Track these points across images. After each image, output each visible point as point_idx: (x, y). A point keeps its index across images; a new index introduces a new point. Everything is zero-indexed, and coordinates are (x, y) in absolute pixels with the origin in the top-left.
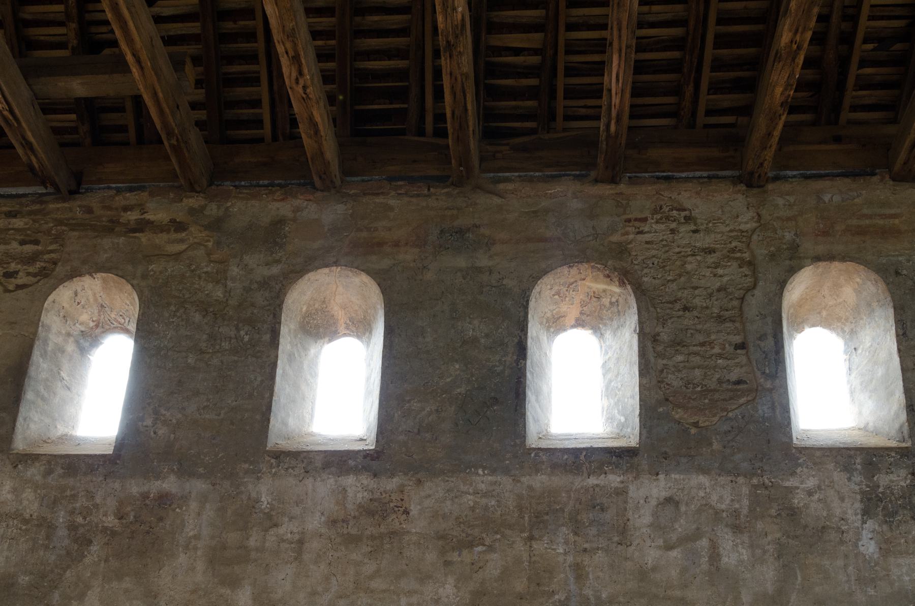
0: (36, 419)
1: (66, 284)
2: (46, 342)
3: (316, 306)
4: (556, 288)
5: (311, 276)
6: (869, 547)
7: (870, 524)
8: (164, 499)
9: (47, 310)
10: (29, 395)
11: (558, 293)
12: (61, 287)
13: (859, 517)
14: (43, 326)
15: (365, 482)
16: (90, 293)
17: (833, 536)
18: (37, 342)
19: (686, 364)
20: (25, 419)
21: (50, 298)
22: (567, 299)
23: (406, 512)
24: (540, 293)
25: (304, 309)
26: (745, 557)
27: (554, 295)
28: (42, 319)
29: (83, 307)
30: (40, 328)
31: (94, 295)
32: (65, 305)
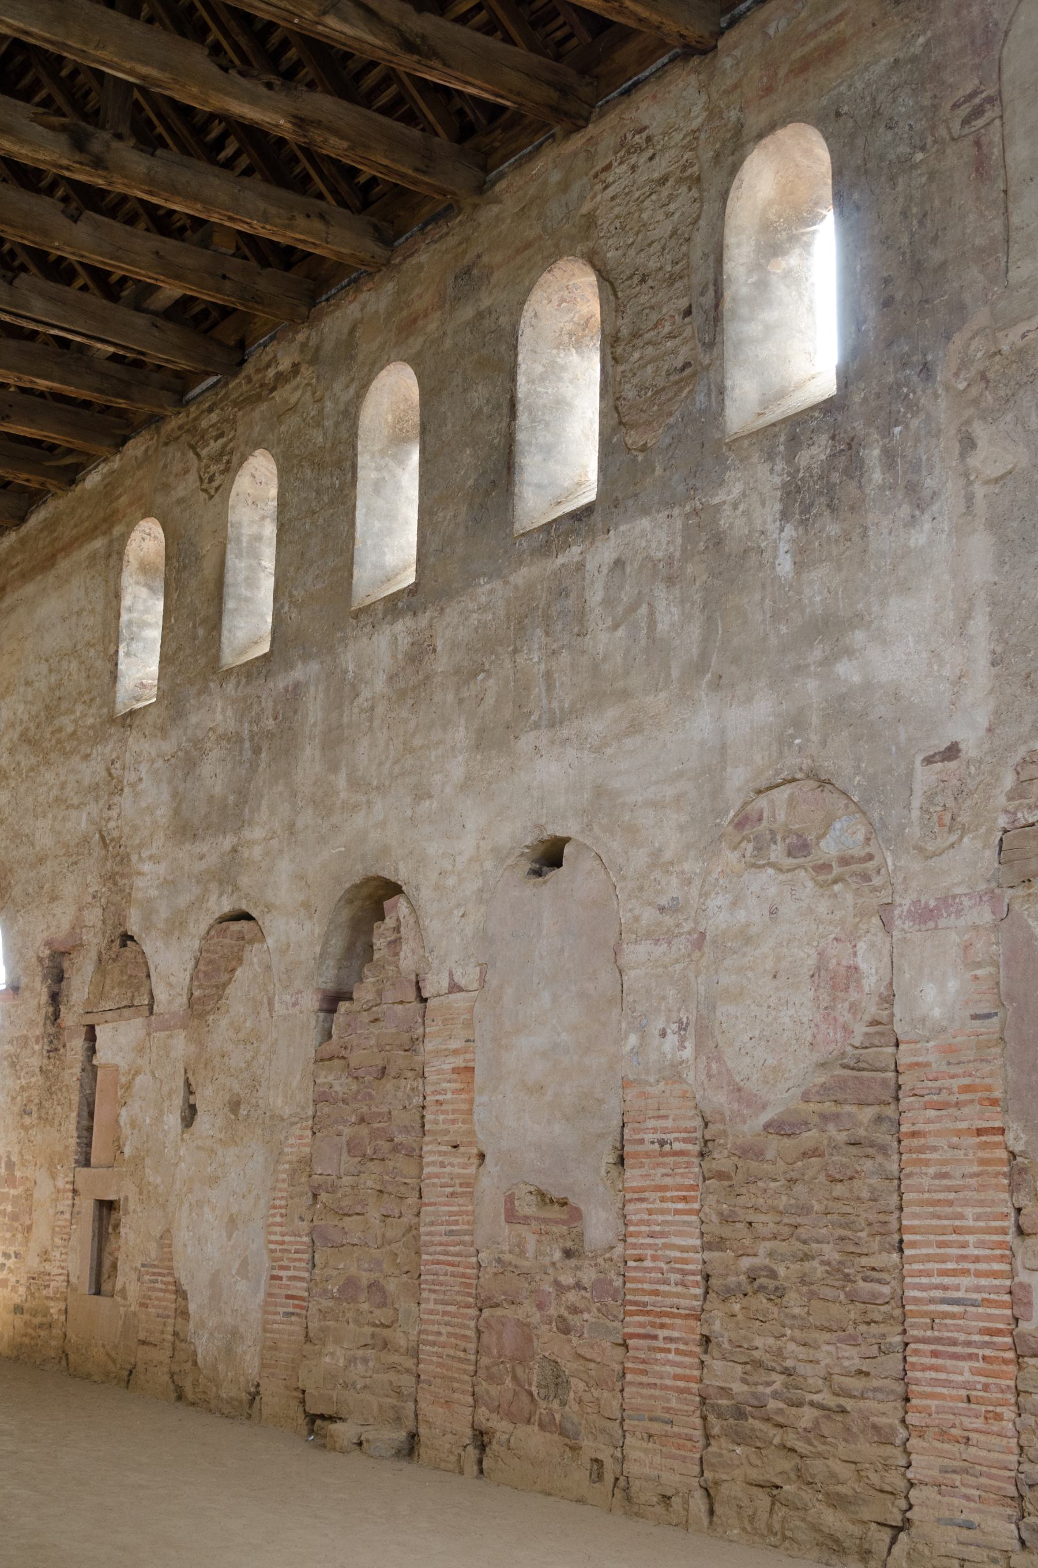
0: (243, 625)
1: (240, 473)
2: (238, 540)
3: (402, 407)
4: (555, 298)
5: (375, 384)
6: (785, 566)
7: (789, 531)
8: (297, 685)
9: (234, 507)
10: (230, 604)
11: (563, 300)
12: (237, 478)
13: (778, 523)
14: (232, 526)
15: (408, 624)
16: (263, 469)
17: (753, 560)
18: (229, 546)
19: (641, 362)
20: (230, 631)
21: (233, 493)
22: (578, 299)
23: (434, 650)
24: (536, 315)
25: (390, 418)
26: (676, 618)
27: (559, 305)
28: (230, 518)
29: (267, 484)
30: (229, 530)
31: (267, 469)
32: (249, 491)
